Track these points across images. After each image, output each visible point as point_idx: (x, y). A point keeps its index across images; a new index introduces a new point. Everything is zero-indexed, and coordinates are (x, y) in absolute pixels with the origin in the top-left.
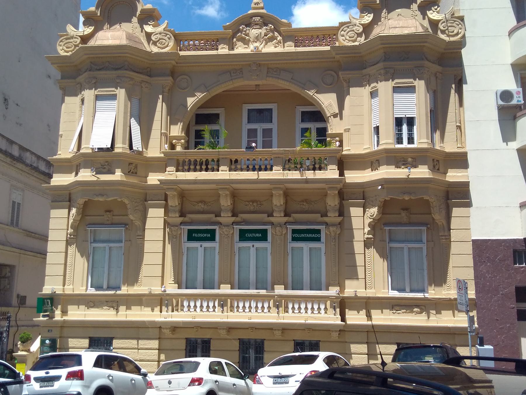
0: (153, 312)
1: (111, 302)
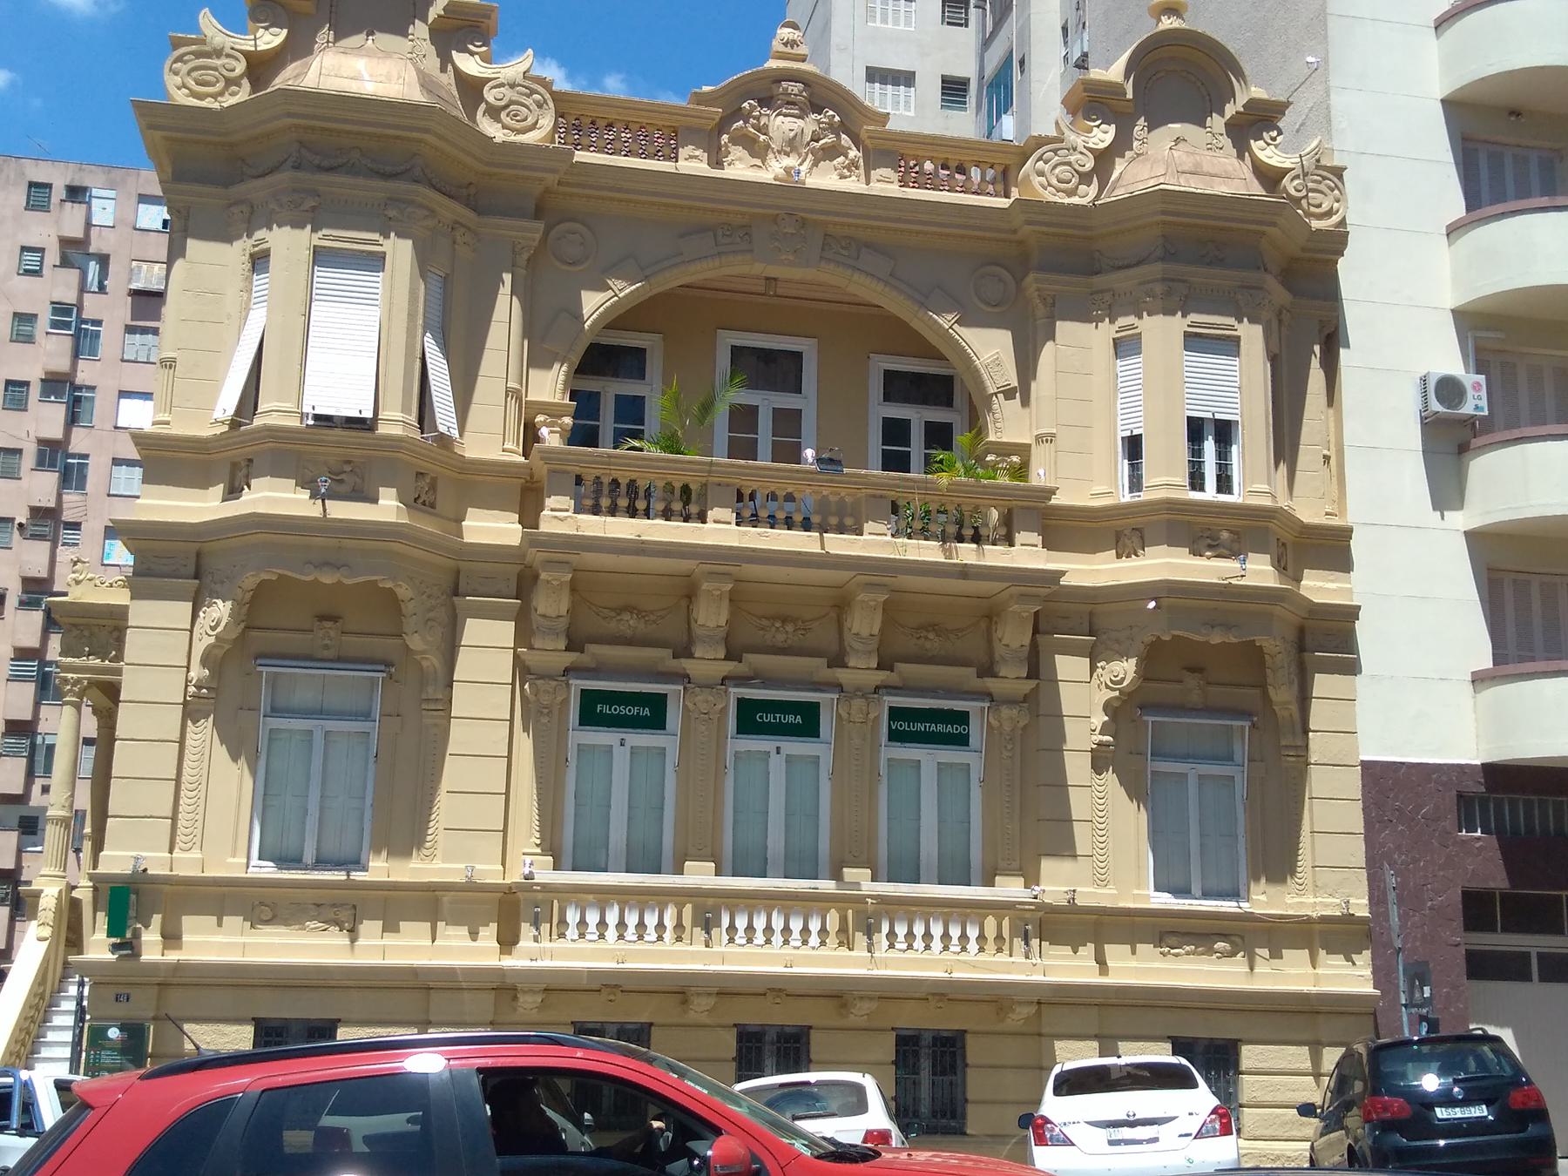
0: (474, 940)
1: (334, 905)
